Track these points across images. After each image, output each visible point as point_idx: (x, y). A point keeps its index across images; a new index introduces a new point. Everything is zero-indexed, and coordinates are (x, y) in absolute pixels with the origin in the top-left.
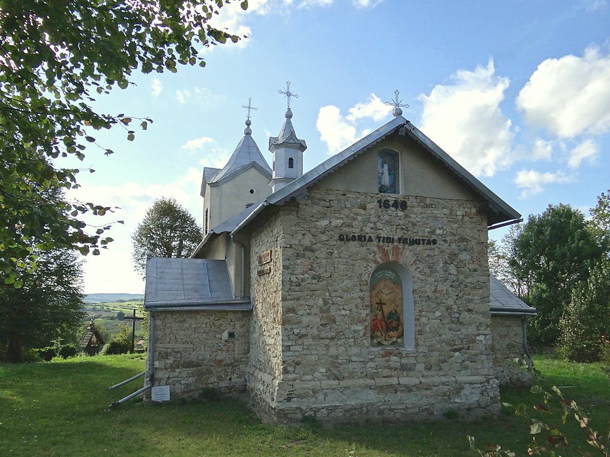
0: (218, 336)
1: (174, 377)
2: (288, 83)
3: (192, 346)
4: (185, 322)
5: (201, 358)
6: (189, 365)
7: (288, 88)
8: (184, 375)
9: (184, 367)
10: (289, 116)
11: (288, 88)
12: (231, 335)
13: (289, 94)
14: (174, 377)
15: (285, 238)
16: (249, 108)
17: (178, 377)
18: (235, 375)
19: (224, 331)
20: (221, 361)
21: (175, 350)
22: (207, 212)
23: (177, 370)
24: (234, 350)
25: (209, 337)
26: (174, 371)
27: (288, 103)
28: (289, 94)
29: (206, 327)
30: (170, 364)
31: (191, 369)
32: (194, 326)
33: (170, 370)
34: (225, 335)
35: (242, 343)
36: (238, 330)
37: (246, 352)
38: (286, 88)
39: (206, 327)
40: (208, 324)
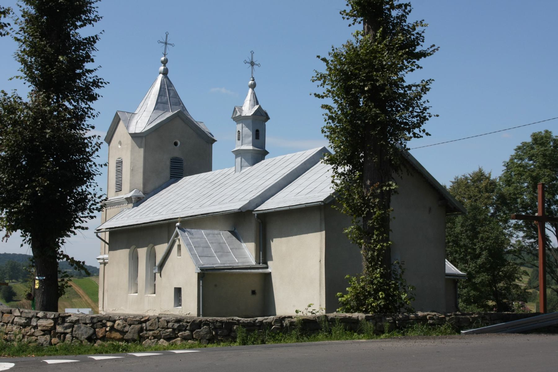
2: (252, 53)
13: (252, 64)
16: (166, 43)
27: (252, 73)
28: (252, 64)
38: (250, 58)
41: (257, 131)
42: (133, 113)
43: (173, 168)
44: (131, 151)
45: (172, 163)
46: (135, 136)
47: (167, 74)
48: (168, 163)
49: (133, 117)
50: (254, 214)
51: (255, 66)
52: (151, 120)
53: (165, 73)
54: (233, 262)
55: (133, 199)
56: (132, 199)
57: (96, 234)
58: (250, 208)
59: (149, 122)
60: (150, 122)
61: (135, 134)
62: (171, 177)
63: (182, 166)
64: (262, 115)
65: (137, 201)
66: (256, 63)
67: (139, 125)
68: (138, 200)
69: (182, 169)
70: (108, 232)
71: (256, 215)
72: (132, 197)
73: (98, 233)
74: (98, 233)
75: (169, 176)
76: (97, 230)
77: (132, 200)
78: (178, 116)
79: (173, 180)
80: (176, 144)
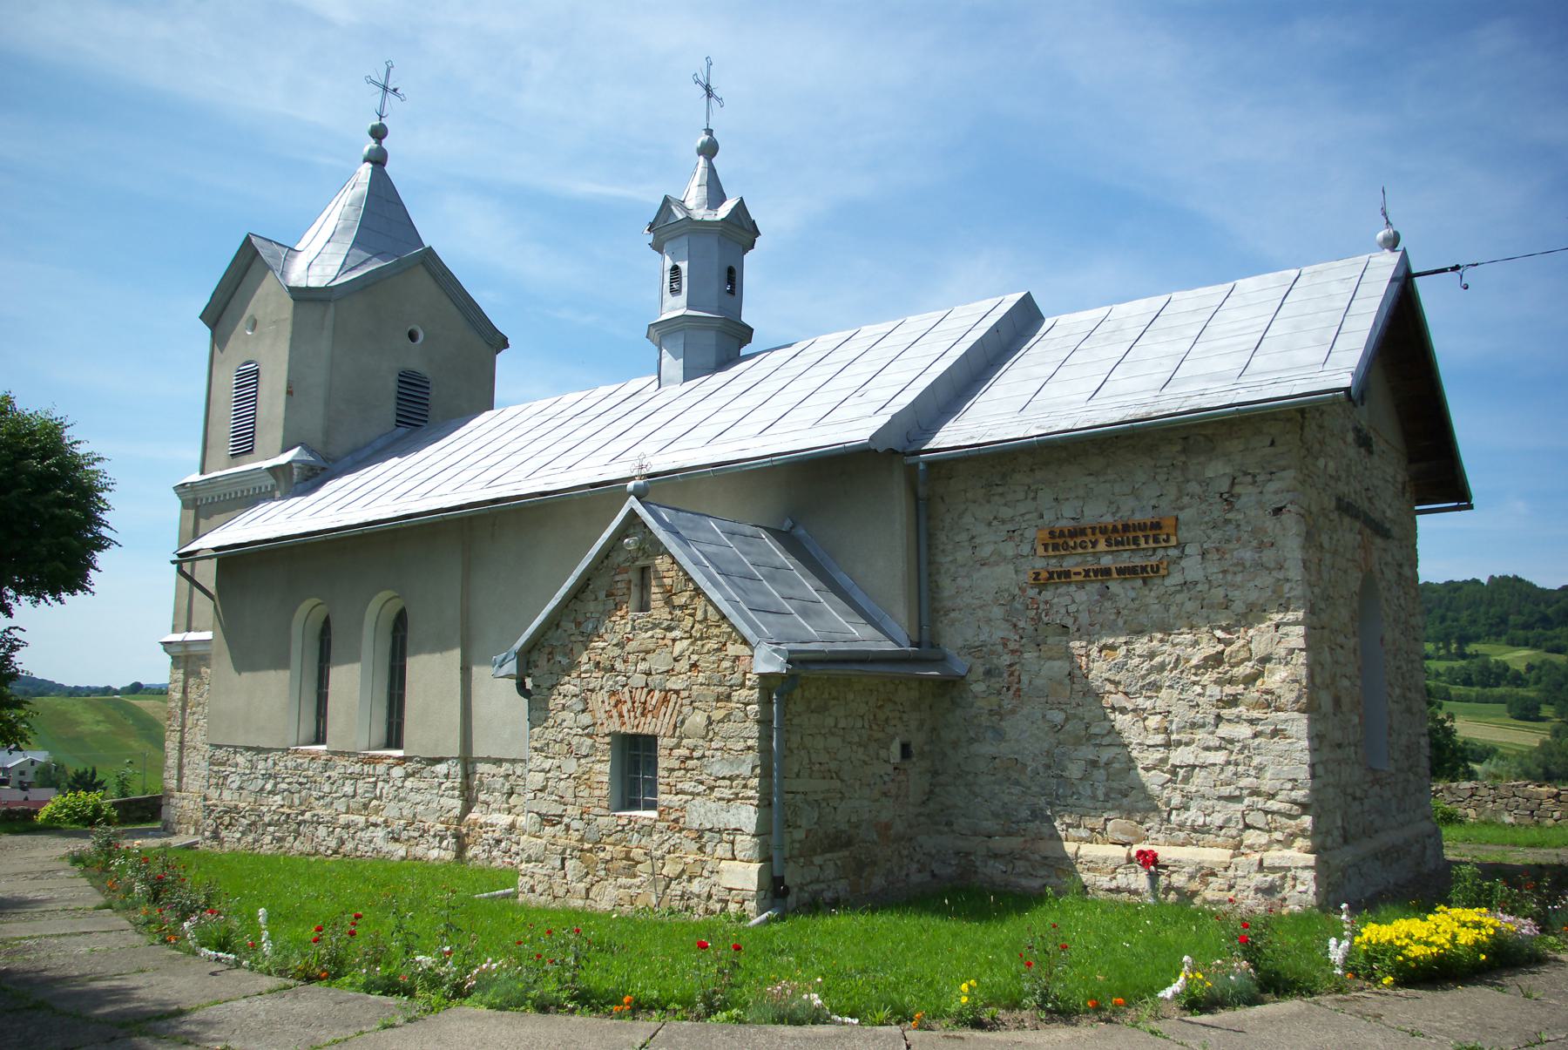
0: (883, 753)
1: (811, 882)
3: (838, 784)
4: (827, 713)
5: (854, 819)
6: (838, 842)
7: (708, 73)
8: (830, 872)
9: (824, 852)
10: (709, 150)
11: (708, 73)
12: (906, 750)
14: (811, 882)
15: (1295, 490)
17: (818, 881)
18: (915, 866)
19: (893, 738)
20: (888, 826)
21: (810, 798)
22: (249, 379)
23: (818, 860)
24: (907, 796)
25: (867, 759)
26: (812, 863)
29: (863, 727)
30: (800, 842)
31: (840, 854)
32: (842, 724)
33: (802, 860)
34: (896, 748)
35: (920, 773)
36: (917, 740)
37: (925, 798)
38: (705, 75)
39: (863, 727)
40: (866, 718)
41: (731, 271)
42: (290, 248)
43: (402, 398)
44: (293, 340)
45: (401, 385)
46: (303, 296)
47: (384, 165)
48: (392, 385)
49: (293, 257)
50: (916, 465)
51: (712, 99)
52: (350, 264)
53: (378, 160)
54: (849, 636)
55: (295, 472)
56: (292, 468)
57: (176, 565)
58: (896, 443)
59: (347, 267)
60: (345, 268)
61: (308, 289)
62: (397, 421)
63: (426, 396)
64: (742, 228)
65: (306, 479)
66: (716, 92)
67: (315, 270)
68: (310, 474)
69: (427, 405)
70: (215, 560)
71: (922, 466)
72: (294, 465)
73: (184, 564)
74: (184, 564)
75: (392, 418)
76: (180, 555)
77: (292, 474)
78: (423, 263)
79: (402, 430)
80: (412, 336)
